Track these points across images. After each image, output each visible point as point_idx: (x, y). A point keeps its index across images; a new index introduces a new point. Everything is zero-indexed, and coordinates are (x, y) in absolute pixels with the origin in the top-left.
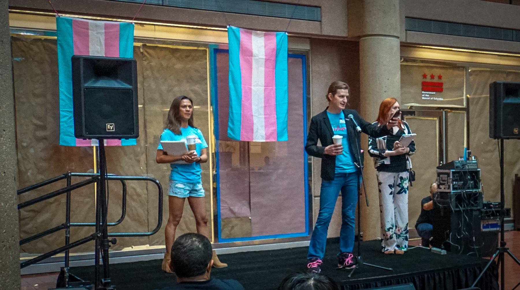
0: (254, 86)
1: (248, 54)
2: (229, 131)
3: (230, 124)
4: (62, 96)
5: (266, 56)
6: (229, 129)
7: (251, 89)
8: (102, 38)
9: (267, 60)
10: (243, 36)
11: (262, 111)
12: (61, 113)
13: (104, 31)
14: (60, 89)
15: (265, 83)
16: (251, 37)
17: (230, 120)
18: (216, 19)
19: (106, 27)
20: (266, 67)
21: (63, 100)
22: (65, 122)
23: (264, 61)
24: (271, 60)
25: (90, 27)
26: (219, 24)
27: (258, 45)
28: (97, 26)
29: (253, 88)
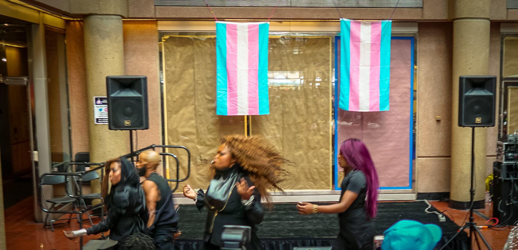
0: (362, 66)
1: (356, 40)
2: (340, 103)
3: (341, 98)
4: (219, 80)
5: (372, 41)
6: (340, 101)
7: (358, 69)
8: (246, 35)
9: (372, 44)
10: (353, 26)
11: (368, 87)
12: (218, 91)
13: (247, 30)
14: (218, 75)
15: (371, 63)
16: (360, 27)
17: (341, 95)
18: (332, 14)
19: (249, 27)
20: (372, 50)
21: (220, 82)
22: (219, 98)
23: (370, 45)
24: (376, 44)
25: (238, 28)
26: (334, 18)
27: (366, 32)
28: (243, 27)
29: (361, 68)
